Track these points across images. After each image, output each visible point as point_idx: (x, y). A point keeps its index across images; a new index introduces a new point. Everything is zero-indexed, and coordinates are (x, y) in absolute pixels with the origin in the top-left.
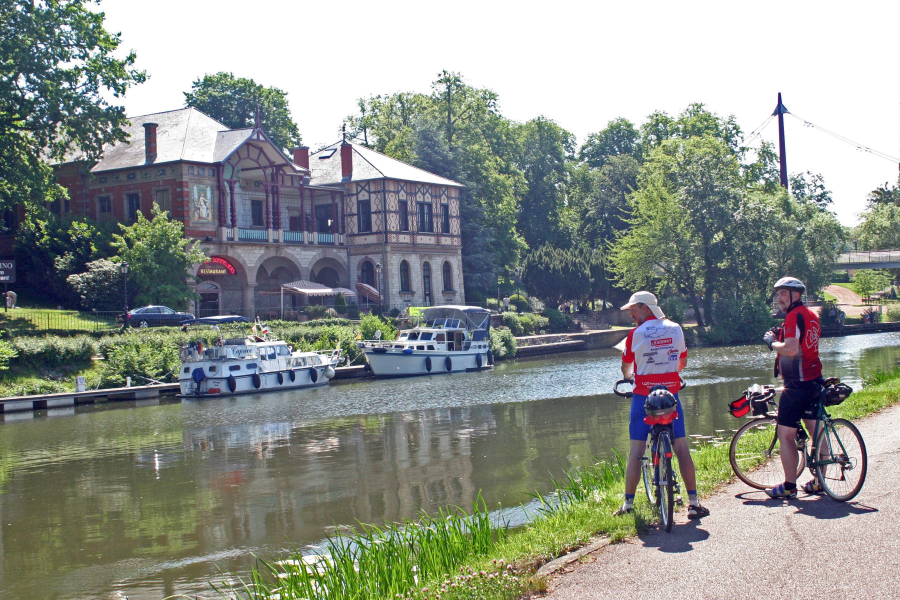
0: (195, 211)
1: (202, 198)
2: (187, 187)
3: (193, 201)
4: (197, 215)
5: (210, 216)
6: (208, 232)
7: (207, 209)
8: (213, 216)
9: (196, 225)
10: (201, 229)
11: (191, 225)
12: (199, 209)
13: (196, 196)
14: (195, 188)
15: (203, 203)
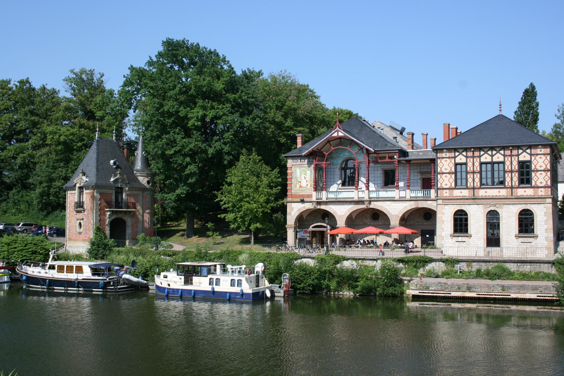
0: (296, 184)
1: (303, 176)
2: (291, 170)
3: (296, 178)
4: (298, 186)
5: (309, 185)
6: (306, 195)
7: (307, 181)
8: (311, 186)
9: (297, 192)
10: (300, 194)
11: (293, 192)
12: (300, 182)
13: (298, 175)
14: (298, 170)
15: (303, 178)
